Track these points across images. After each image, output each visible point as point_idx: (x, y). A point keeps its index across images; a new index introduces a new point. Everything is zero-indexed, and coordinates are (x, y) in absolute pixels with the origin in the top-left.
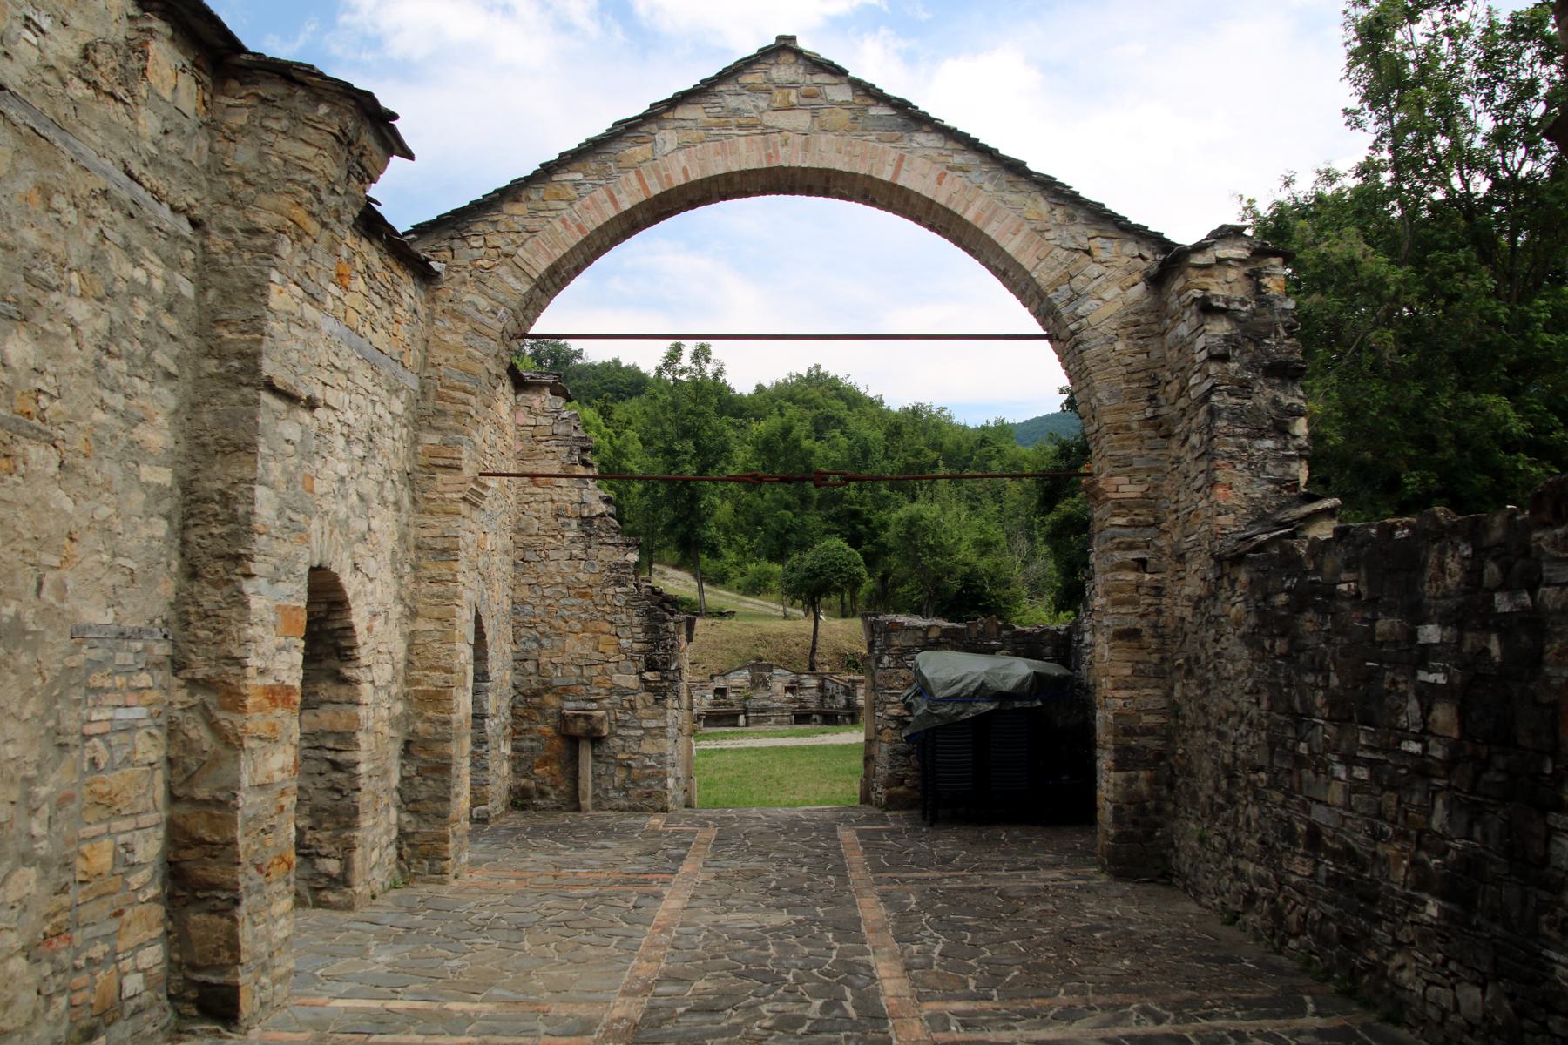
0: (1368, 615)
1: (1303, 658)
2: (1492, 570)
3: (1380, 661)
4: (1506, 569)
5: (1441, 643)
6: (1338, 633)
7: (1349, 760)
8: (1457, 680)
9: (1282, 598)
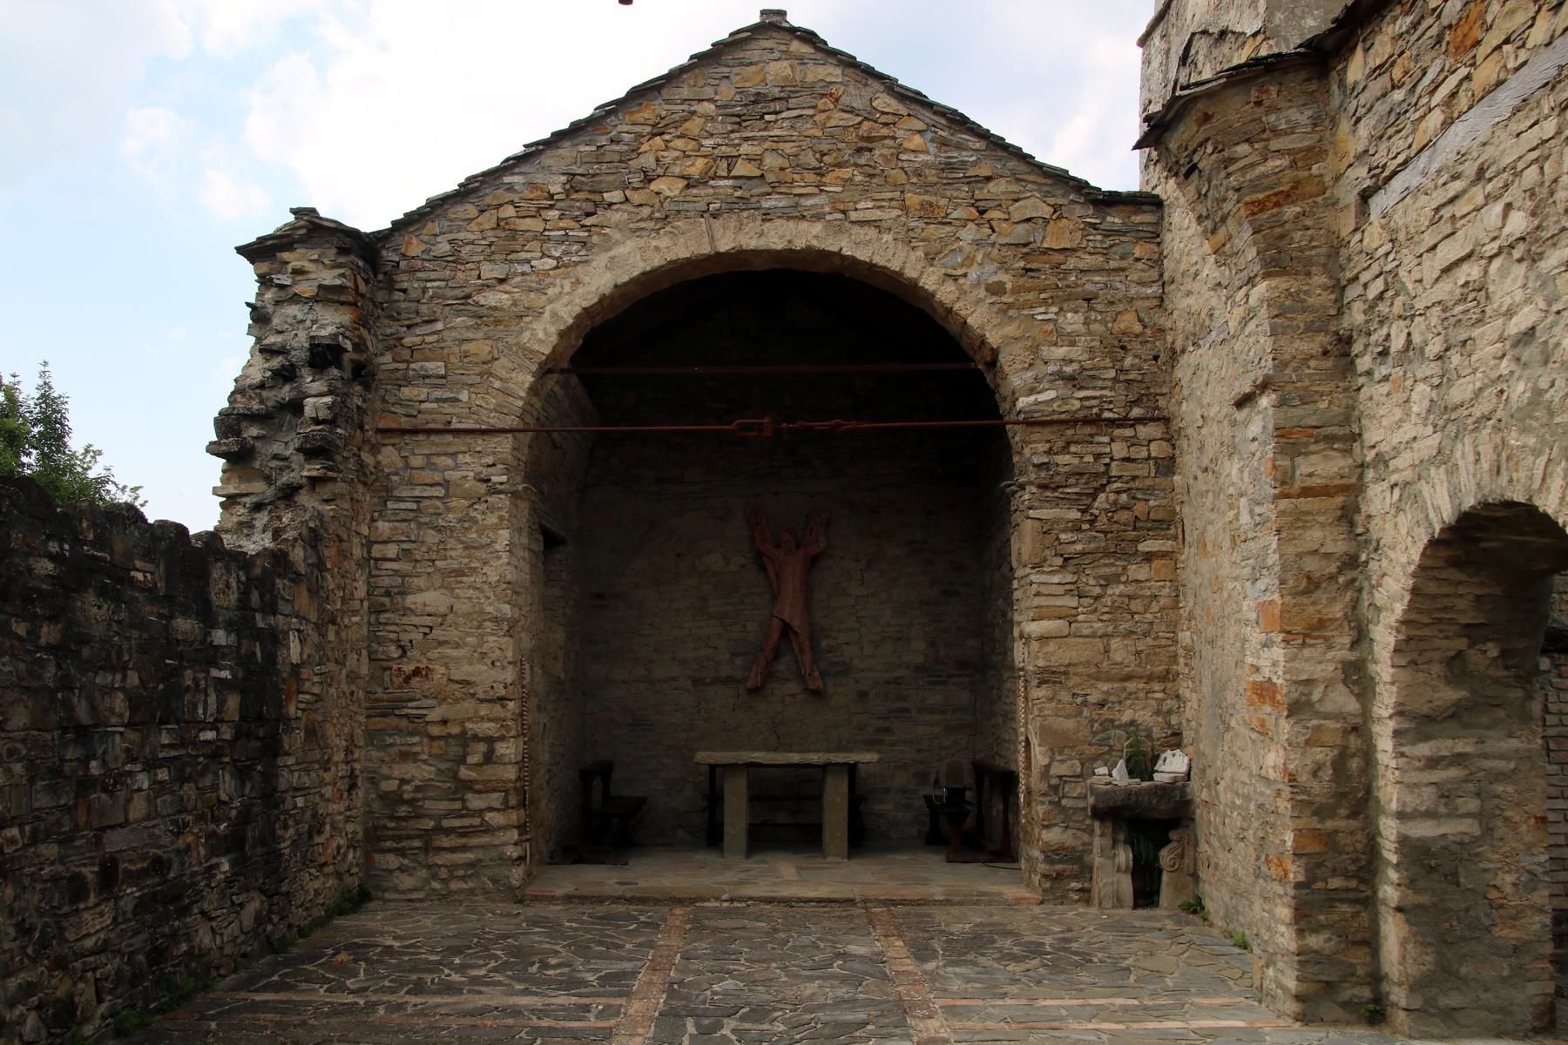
0: (166, 612)
1: (86, 652)
2: (255, 598)
3: (180, 657)
4: (262, 596)
5: (227, 646)
6: (132, 626)
7: (151, 765)
8: (240, 675)
9: (46, 567)
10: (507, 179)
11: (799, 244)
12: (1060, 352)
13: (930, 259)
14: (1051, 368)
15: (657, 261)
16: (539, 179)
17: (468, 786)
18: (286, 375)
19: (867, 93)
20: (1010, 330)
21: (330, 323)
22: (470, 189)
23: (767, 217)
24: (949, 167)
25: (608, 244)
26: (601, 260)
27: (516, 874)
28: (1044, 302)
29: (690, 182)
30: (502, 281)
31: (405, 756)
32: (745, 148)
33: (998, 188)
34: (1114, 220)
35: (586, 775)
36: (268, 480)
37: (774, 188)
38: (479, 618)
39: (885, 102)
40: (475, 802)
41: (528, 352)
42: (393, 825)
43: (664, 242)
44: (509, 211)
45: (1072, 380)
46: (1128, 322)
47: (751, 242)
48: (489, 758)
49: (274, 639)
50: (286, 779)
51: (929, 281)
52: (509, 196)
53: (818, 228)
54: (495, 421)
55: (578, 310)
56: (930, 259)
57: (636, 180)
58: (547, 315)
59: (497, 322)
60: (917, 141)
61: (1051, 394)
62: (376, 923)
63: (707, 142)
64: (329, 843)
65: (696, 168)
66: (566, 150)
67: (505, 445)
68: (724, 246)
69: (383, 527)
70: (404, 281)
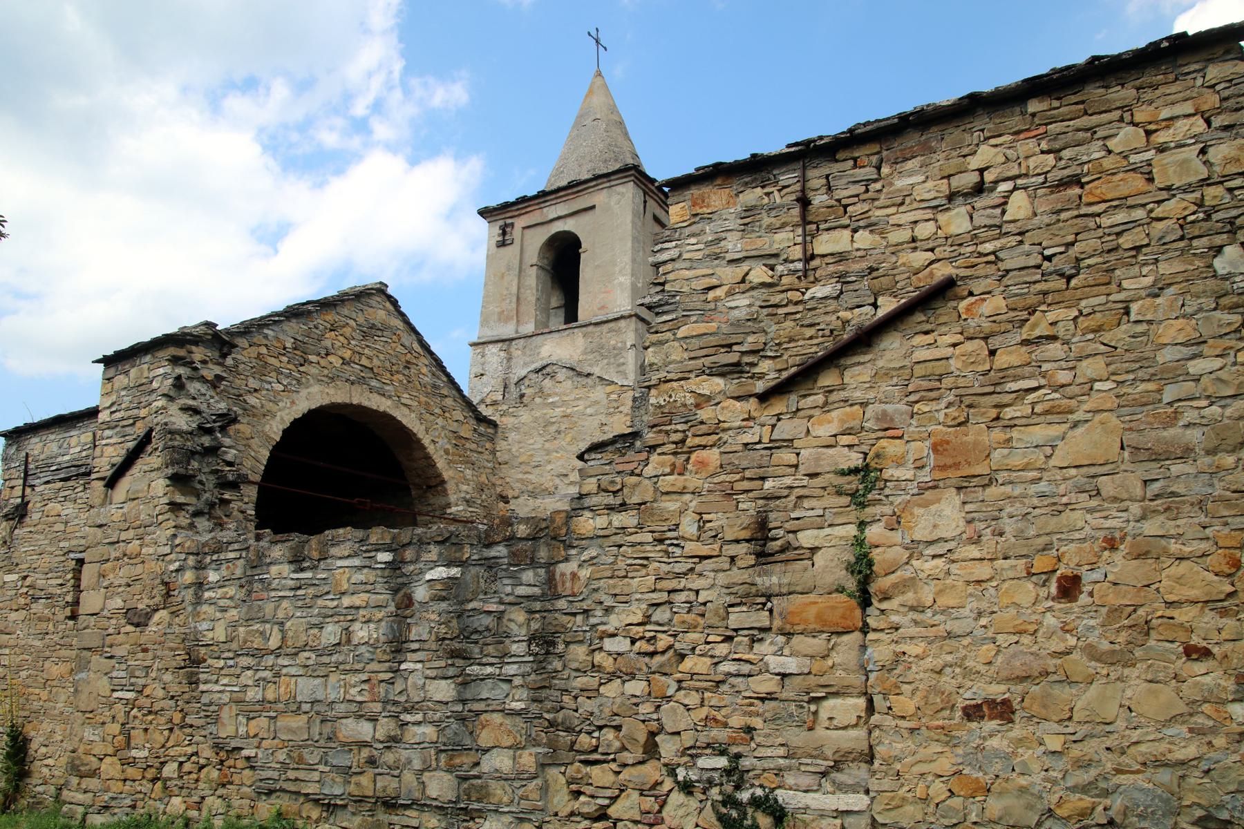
10: (266, 331)
11: (382, 409)
12: (465, 488)
14: (463, 495)
15: (326, 401)
16: (281, 336)
19: (410, 338)
20: (451, 473)
24: (435, 386)
26: (304, 392)
28: (461, 462)
29: (345, 362)
30: (256, 390)
32: (366, 351)
33: (449, 402)
34: (482, 429)
36: (198, 497)
37: (376, 376)
39: (416, 346)
43: (332, 391)
44: (264, 350)
45: (467, 501)
46: (483, 478)
47: (366, 403)
51: (426, 441)
52: (265, 342)
53: (389, 402)
55: (292, 419)
56: (427, 431)
57: (323, 352)
58: (278, 418)
59: (254, 416)
60: (424, 370)
61: (461, 508)
63: (353, 342)
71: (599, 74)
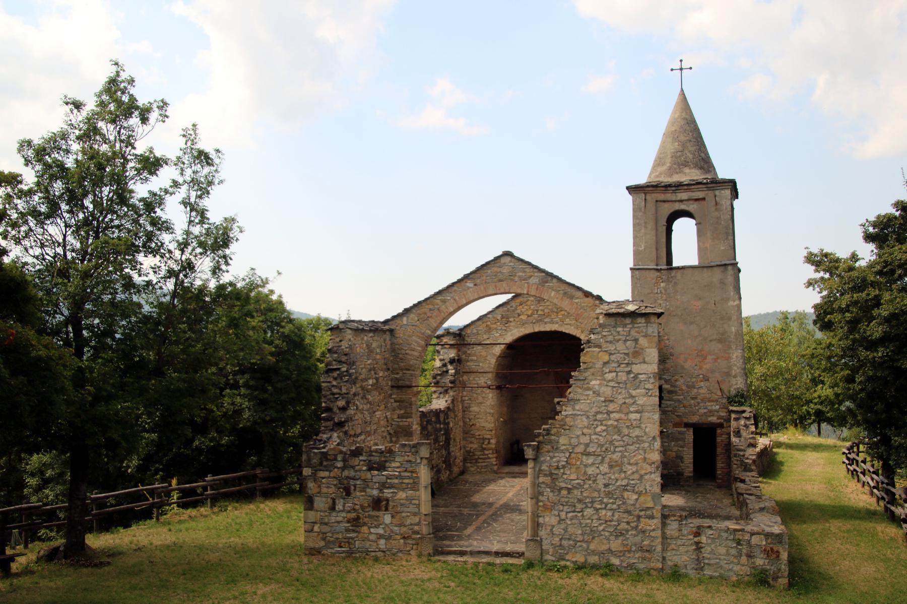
13: (582, 332)
15: (521, 334)
17: (484, 449)
18: (445, 365)
21: (452, 354)
22: (479, 319)
23: (546, 323)
25: (511, 330)
26: (509, 334)
27: (495, 468)
31: (471, 443)
35: (512, 445)
38: (486, 413)
40: (486, 452)
41: (494, 354)
42: (469, 457)
43: (523, 330)
47: (542, 329)
48: (489, 443)
49: (448, 423)
50: (451, 449)
54: (488, 370)
56: (582, 332)
62: (466, 477)
64: (457, 461)
65: (530, 312)
66: (501, 309)
67: (490, 375)
68: (536, 330)
69: (465, 393)
70: (466, 339)
71: (682, 90)
